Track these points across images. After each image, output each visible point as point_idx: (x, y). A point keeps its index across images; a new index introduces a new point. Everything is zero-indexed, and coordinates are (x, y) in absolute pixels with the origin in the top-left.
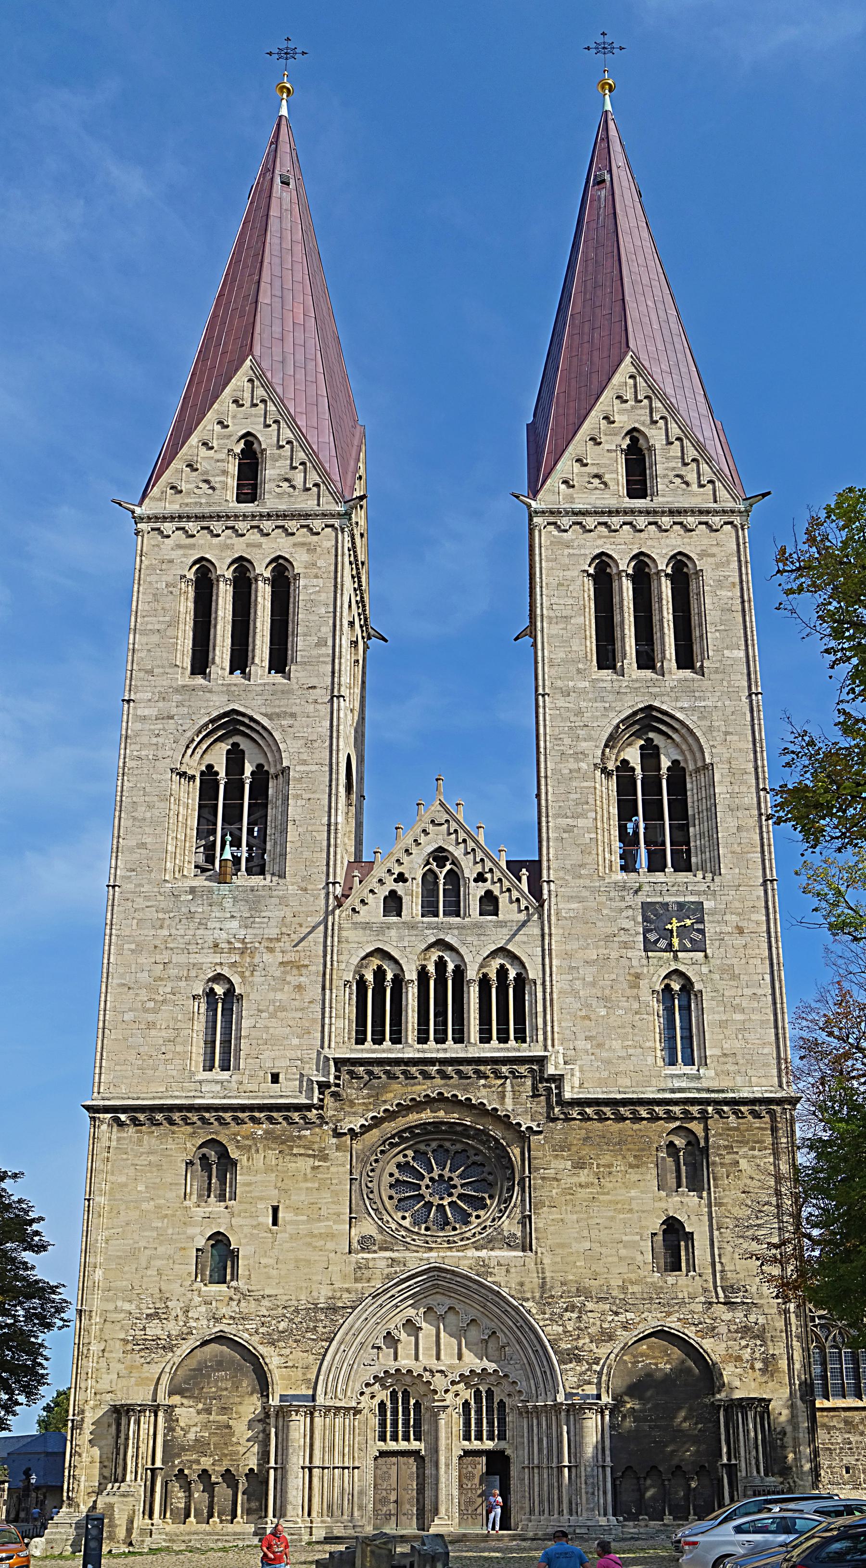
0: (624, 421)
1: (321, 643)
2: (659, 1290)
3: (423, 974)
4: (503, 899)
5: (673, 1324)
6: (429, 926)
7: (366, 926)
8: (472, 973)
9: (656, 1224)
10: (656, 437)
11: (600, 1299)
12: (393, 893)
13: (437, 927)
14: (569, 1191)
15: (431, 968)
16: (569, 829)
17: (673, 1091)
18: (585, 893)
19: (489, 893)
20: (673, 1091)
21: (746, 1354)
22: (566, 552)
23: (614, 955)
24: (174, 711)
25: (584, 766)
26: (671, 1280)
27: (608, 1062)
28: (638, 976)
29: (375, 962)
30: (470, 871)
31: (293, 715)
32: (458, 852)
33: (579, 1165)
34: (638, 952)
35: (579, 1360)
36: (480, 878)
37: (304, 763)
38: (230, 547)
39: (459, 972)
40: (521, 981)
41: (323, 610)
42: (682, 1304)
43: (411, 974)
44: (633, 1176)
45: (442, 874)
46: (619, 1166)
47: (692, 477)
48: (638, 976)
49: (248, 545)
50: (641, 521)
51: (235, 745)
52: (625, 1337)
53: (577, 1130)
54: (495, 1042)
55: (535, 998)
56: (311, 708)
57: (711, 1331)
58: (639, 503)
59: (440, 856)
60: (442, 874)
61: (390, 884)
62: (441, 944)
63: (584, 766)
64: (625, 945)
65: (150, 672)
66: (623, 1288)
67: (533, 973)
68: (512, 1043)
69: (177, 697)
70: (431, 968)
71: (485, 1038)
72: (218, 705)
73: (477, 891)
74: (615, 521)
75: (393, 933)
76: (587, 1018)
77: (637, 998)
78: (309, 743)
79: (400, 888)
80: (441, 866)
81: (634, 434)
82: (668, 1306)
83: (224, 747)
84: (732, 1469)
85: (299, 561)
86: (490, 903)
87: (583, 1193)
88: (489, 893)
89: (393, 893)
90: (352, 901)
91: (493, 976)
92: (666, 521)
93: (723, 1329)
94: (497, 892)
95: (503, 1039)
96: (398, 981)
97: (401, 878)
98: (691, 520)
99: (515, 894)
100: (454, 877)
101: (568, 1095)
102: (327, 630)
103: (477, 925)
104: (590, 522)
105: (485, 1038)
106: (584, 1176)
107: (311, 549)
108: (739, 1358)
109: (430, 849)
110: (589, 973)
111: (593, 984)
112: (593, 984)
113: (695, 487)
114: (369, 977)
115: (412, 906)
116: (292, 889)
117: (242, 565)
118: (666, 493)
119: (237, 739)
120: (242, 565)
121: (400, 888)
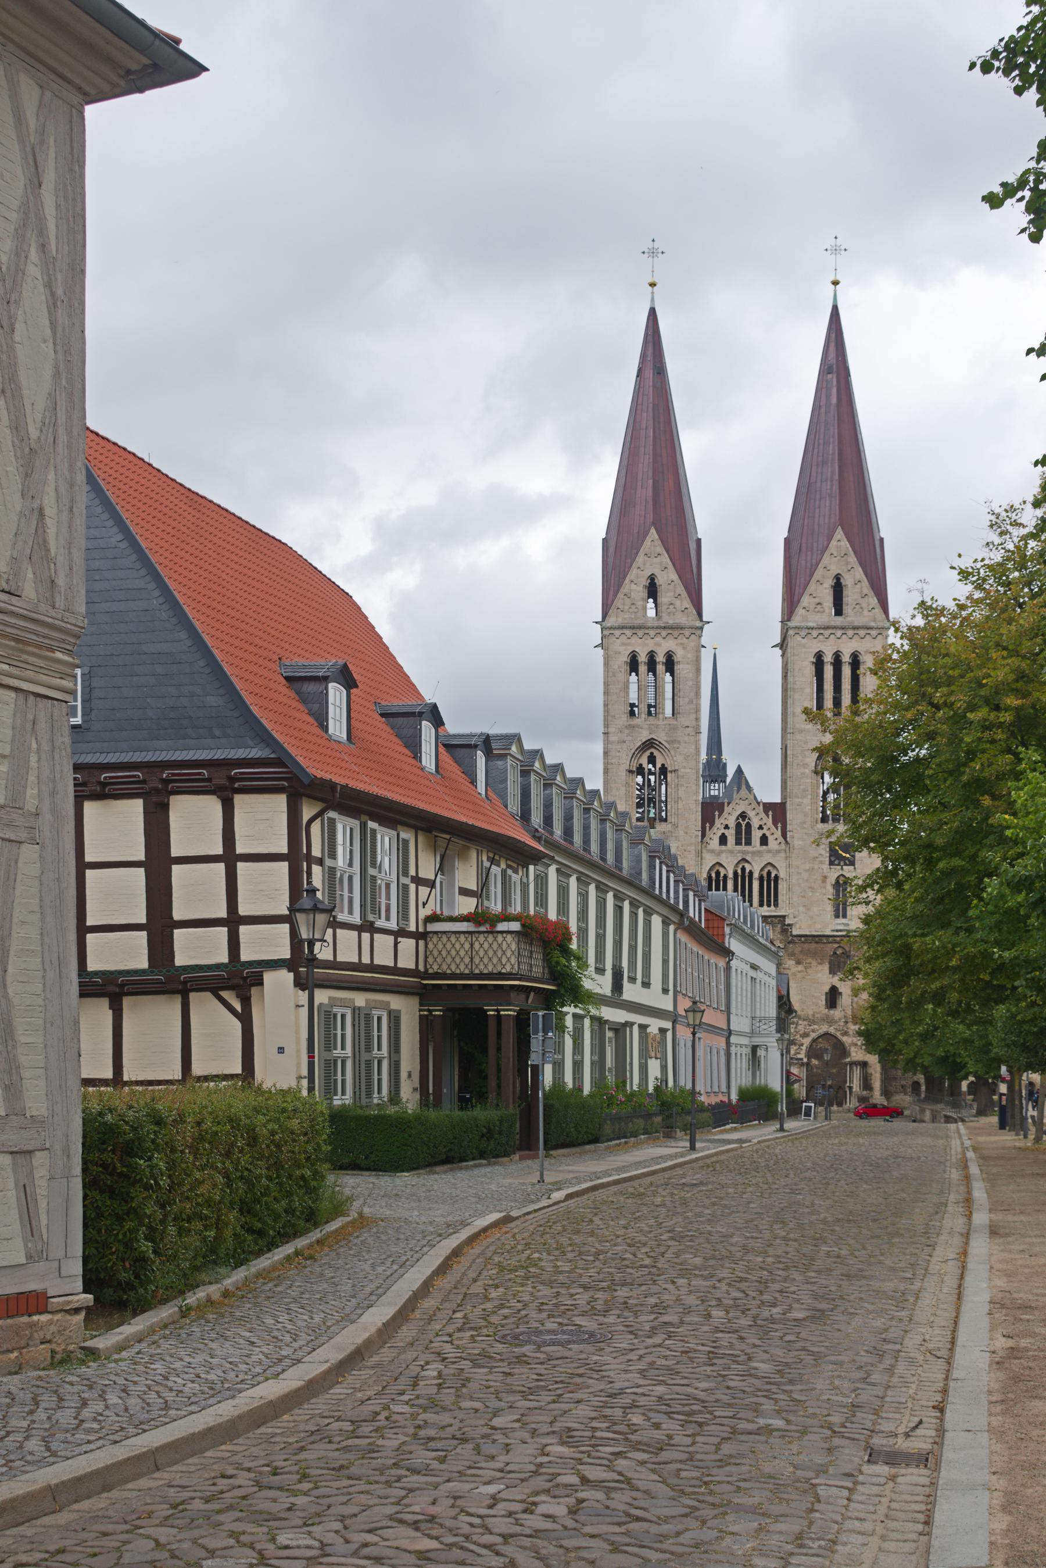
0: (834, 570)
1: (691, 702)
2: (827, 1016)
3: (735, 873)
4: (771, 839)
5: (832, 1030)
6: (739, 852)
7: (712, 852)
8: (756, 875)
9: (827, 988)
10: (848, 581)
11: (805, 1020)
12: (723, 834)
13: (743, 852)
14: (794, 974)
15: (739, 871)
16: (799, 805)
17: (837, 931)
18: (805, 837)
19: (764, 835)
20: (837, 931)
21: (859, 1043)
22: (804, 650)
23: (816, 867)
24: (626, 738)
25: (807, 771)
26: (832, 1012)
27: (811, 918)
28: (825, 877)
29: (717, 867)
30: (755, 823)
31: (679, 742)
32: (751, 814)
33: (798, 963)
34: (826, 866)
35: (795, 1044)
36: (761, 828)
37: (684, 767)
38: (647, 645)
39: (751, 873)
40: (777, 877)
41: (690, 683)
42: (836, 1022)
43: (731, 875)
44: (820, 968)
45: (744, 824)
46: (814, 963)
47: (864, 605)
48: (825, 877)
49: (656, 644)
50: (839, 633)
51: (652, 753)
52: (813, 1035)
53: (797, 948)
54: (765, 906)
55: (782, 886)
56: (686, 738)
57: (846, 1033)
58: (839, 621)
59: (743, 816)
60: (744, 824)
61: (723, 831)
62: (744, 860)
63: (807, 771)
64: (821, 862)
65: (614, 717)
66: (813, 1015)
67: (782, 875)
68: (772, 907)
69: (626, 731)
70: (739, 871)
71: (761, 905)
72: (644, 736)
73: (760, 833)
74: (827, 633)
75: (724, 855)
76: (804, 897)
77: (825, 887)
78: (686, 757)
79: (726, 832)
80: (744, 820)
81: (838, 578)
82: (831, 1022)
83: (648, 753)
84: (850, 1088)
85: (679, 655)
86: (764, 840)
87: (799, 975)
88: (764, 835)
89: (723, 834)
90: (707, 839)
91: (765, 875)
92: (850, 633)
93: (851, 1033)
94: (768, 834)
95: (769, 905)
96: (725, 877)
97: (727, 827)
98: (862, 632)
99: (775, 836)
100: (749, 826)
101: (795, 933)
102: (692, 694)
103: (759, 852)
104: (815, 633)
105: (761, 905)
106: (800, 968)
107: (684, 648)
108: (856, 1045)
109: (739, 812)
110: (805, 875)
111: (807, 881)
112: (807, 881)
113: (866, 612)
114: (713, 875)
115: (731, 840)
116: (681, 833)
117: (652, 655)
118: (851, 615)
119: (653, 750)
120: (652, 655)
121: (726, 832)
